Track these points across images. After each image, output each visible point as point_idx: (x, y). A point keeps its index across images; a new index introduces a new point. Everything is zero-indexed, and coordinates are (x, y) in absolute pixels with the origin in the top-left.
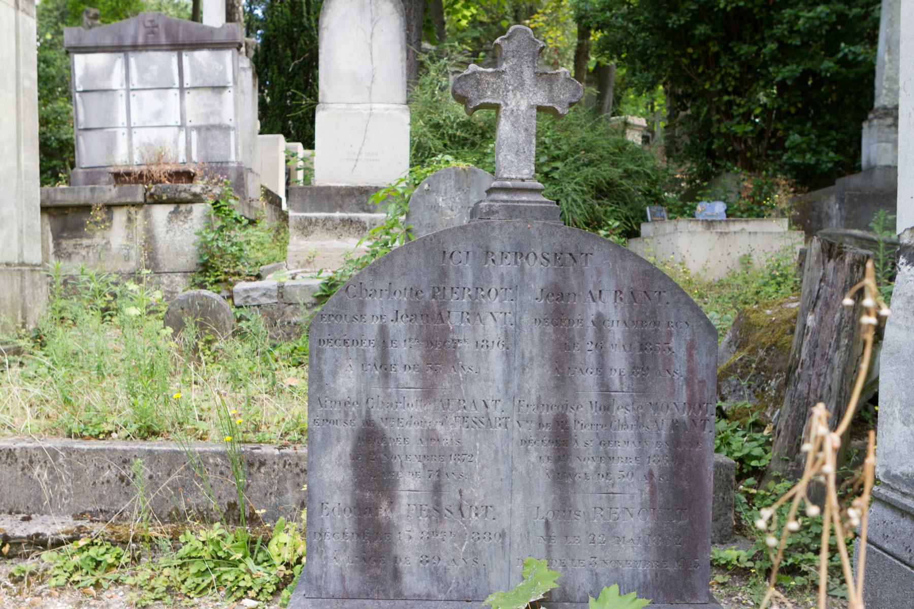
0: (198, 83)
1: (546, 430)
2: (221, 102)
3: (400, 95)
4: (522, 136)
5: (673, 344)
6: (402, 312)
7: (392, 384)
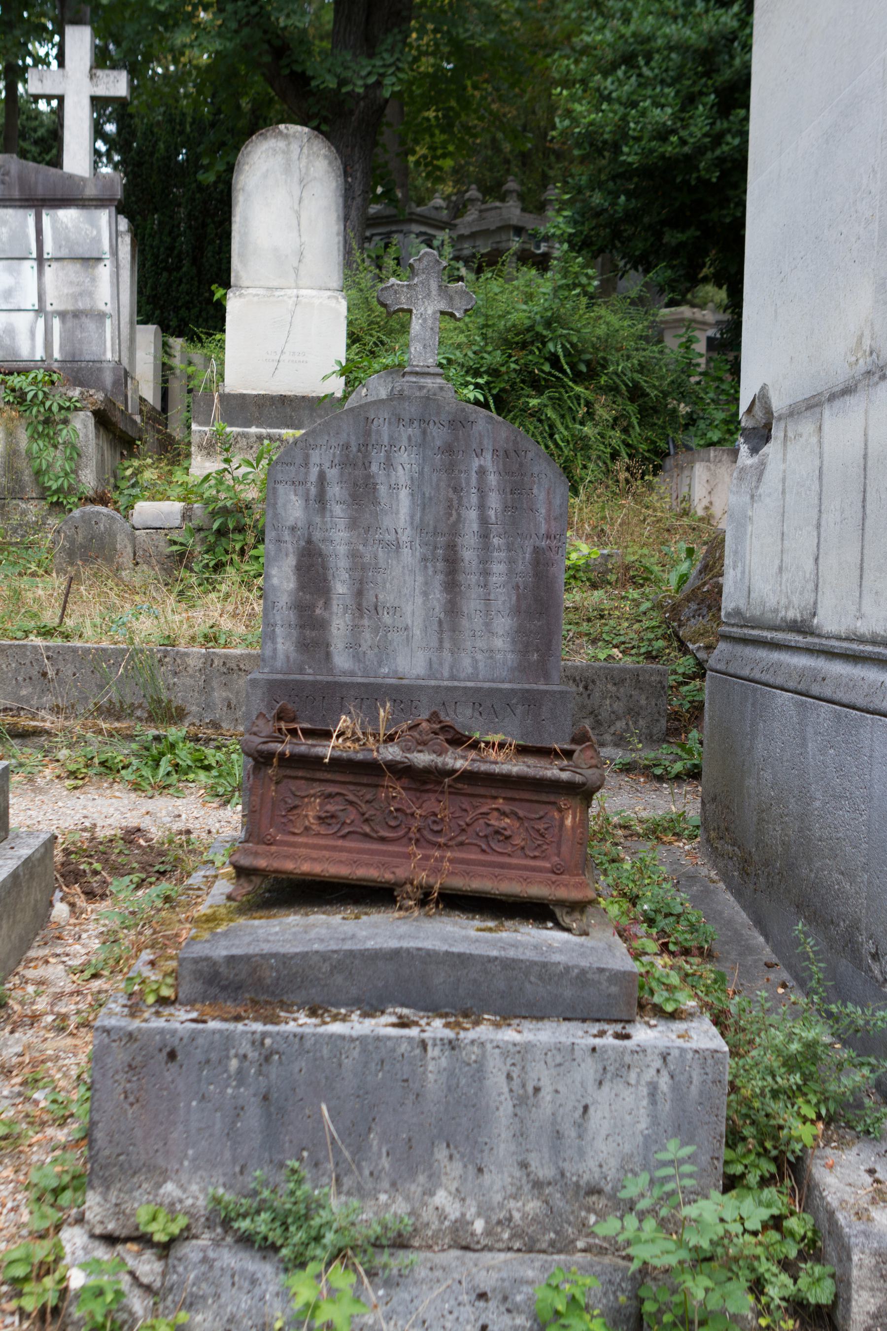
0: (64, 253)
1: (440, 551)
2: (93, 280)
3: (335, 278)
4: (428, 334)
5: (535, 491)
6: (336, 461)
7: (328, 514)
